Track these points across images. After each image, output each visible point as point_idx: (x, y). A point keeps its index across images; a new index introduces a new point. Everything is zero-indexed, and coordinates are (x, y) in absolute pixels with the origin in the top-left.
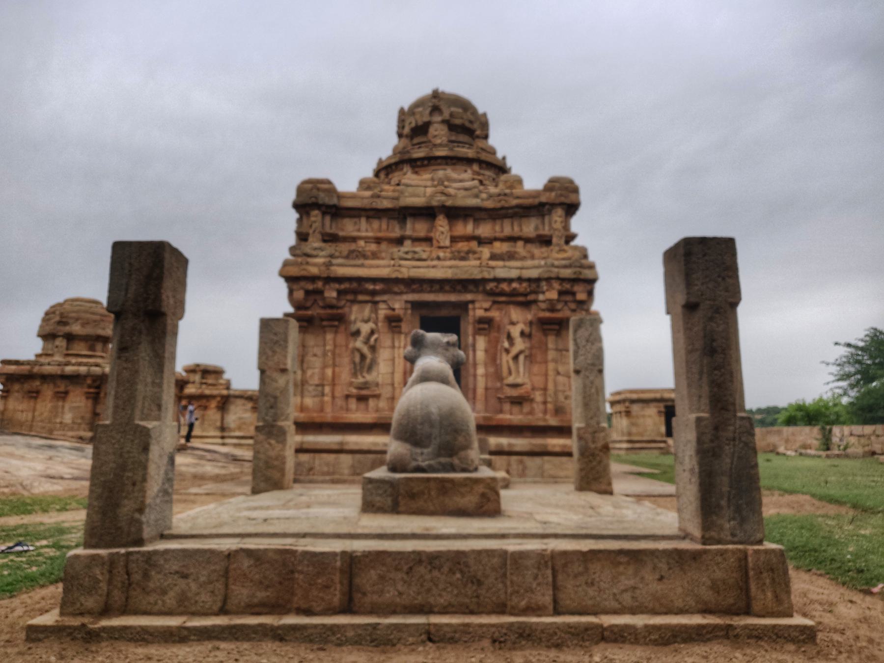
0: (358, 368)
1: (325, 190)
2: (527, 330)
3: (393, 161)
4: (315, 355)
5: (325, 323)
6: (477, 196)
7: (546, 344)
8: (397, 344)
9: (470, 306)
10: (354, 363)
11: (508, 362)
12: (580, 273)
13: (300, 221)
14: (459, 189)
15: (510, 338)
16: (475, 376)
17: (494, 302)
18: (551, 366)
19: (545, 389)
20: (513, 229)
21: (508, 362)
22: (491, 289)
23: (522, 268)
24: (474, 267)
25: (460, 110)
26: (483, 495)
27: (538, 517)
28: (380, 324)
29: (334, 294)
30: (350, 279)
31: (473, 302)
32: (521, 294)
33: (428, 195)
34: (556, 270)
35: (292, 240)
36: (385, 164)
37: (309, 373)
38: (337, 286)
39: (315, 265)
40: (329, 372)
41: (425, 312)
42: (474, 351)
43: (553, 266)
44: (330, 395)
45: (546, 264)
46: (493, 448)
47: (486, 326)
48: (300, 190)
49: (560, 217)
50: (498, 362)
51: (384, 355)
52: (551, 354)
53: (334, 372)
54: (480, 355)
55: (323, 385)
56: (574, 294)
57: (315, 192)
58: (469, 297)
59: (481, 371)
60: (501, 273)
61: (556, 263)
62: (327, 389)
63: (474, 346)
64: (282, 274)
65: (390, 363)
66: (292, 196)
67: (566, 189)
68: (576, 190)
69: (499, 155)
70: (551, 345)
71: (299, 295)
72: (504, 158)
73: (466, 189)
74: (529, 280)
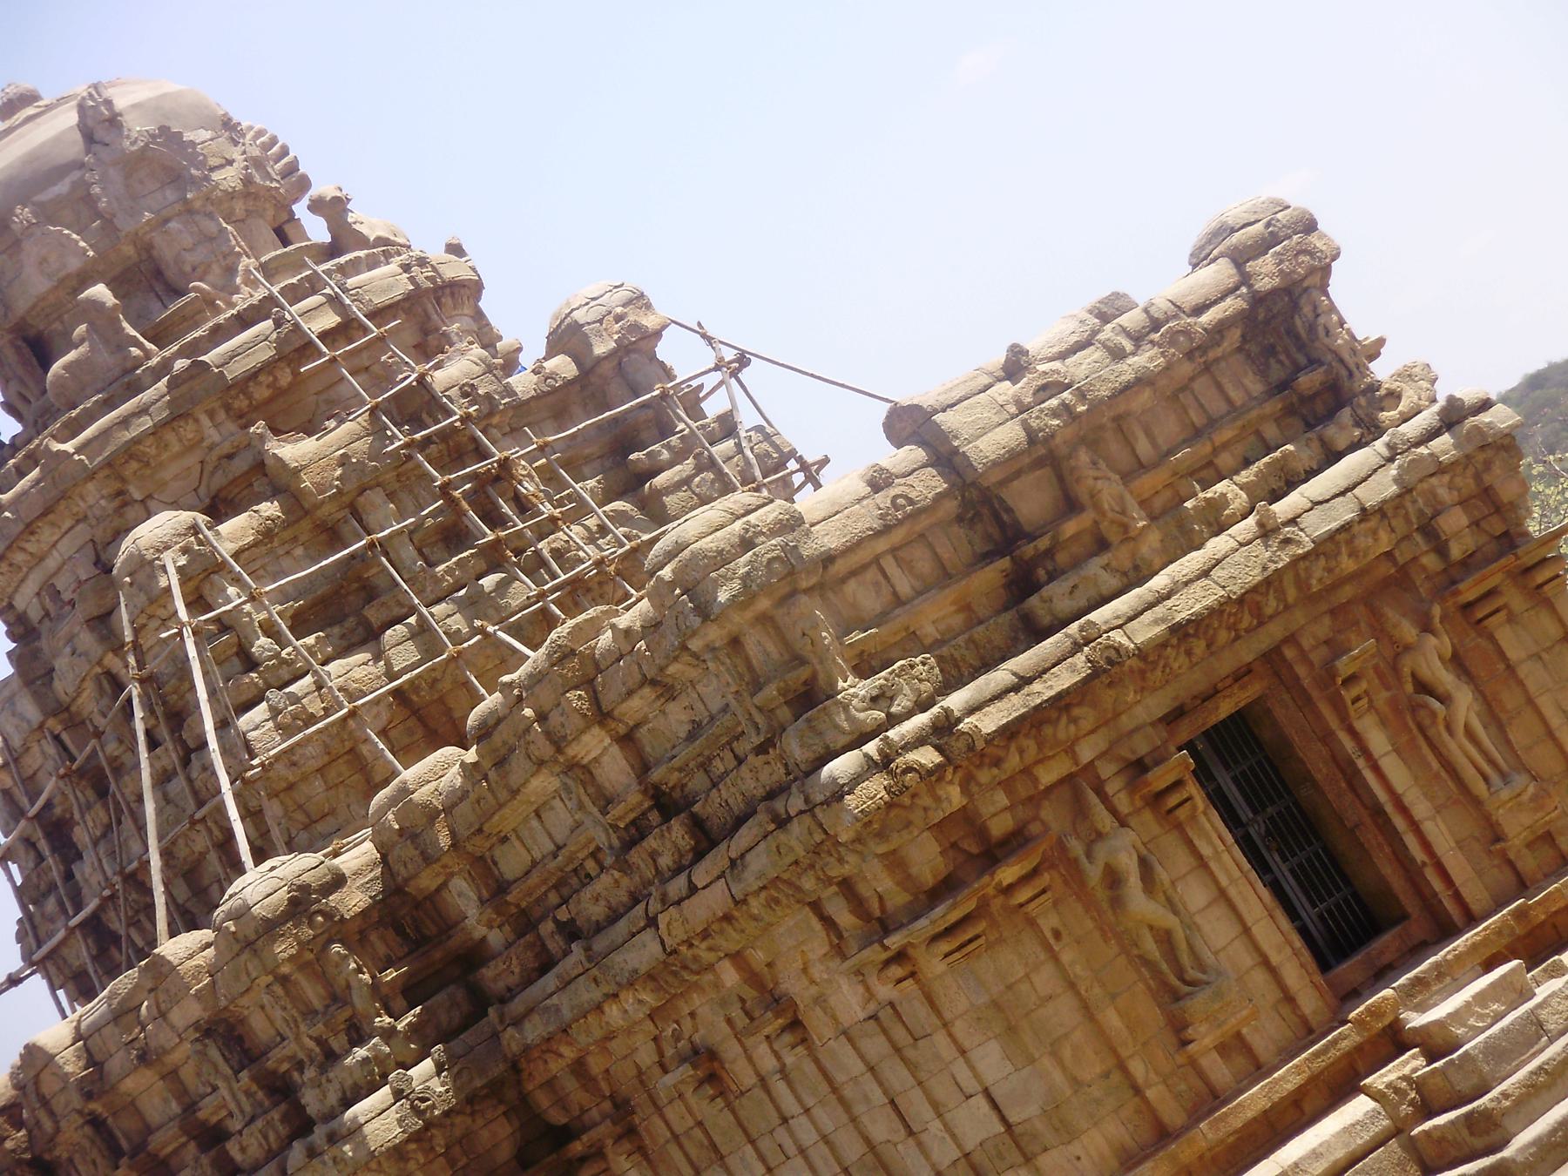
5: (1023, 895)
8: (1206, 851)
9: (1289, 653)
11: (1461, 747)
18: (1546, 704)
21: (1461, 747)
31: (1291, 639)
34: (1423, 450)
37: (1067, 1053)
51: (1195, 895)
59: (1421, 809)
60: (1319, 525)
65: (1220, 910)
70: (1513, 654)
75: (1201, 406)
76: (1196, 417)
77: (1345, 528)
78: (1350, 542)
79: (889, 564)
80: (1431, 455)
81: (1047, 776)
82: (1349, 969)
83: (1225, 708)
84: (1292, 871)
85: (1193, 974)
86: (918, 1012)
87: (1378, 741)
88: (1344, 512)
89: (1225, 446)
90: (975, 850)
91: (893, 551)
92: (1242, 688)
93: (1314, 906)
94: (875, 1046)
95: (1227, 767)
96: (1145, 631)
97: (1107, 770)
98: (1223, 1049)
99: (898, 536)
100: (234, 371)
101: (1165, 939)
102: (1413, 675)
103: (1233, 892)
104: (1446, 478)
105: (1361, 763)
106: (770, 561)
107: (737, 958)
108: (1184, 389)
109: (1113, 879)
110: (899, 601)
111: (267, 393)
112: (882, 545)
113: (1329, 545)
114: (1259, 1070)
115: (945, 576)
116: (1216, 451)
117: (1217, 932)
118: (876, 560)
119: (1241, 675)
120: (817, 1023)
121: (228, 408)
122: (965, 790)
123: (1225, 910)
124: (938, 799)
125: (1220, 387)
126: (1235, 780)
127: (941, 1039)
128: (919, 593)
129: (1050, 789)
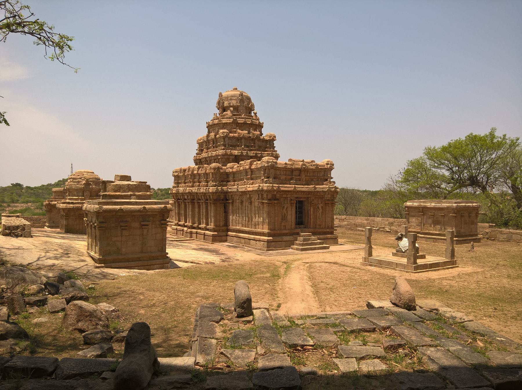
15: (318, 208)
30: (283, 191)
32: (320, 195)
39: (275, 187)
51: (289, 213)
52: (327, 212)
58: (310, 196)
59: (312, 217)
60: (317, 189)
81: (284, 196)
82: (298, 226)
83: (301, 200)
86: (261, 208)
87: (312, 210)
88: (321, 190)
94: (256, 209)
96: (251, 189)
97: (289, 198)
100: (239, 122)
101: (285, 215)
107: (250, 195)
113: (318, 192)
114: (286, 229)
115: (286, 175)
117: (289, 217)
119: (304, 198)
120: (253, 204)
123: (291, 215)
127: (262, 212)
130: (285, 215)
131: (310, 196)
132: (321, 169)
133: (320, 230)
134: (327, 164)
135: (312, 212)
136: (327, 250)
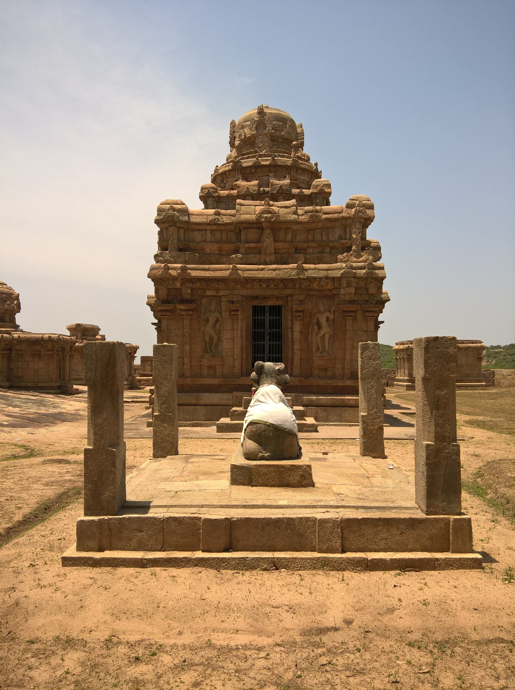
0: (208, 345)
1: (179, 211)
2: (332, 317)
3: (227, 169)
4: (176, 336)
5: (183, 313)
6: (295, 213)
7: (346, 328)
8: (235, 327)
9: (289, 298)
10: (205, 342)
12: (372, 273)
13: (160, 233)
14: (281, 207)
16: (293, 350)
17: (307, 295)
19: (344, 359)
20: (322, 238)
22: (305, 286)
23: (327, 270)
24: (292, 269)
25: (281, 124)
26: (302, 476)
27: (335, 489)
28: (223, 313)
29: (189, 291)
31: (291, 296)
33: (257, 212)
35: (155, 250)
36: (220, 171)
38: (191, 285)
39: (174, 269)
40: (187, 348)
41: (255, 303)
42: (292, 332)
43: (352, 268)
44: (188, 364)
45: (346, 266)
46: (305, 402)
47: (301, 314)
48: (160, 211)
49: (358, 229)
50: (310, 340)
51: (226, 335)
53: (190, 347)
54: (297, 335)
55: (183, 358)
56: (367, 289)
57: (171, 212)
59: (297, 346)
61: (354, 265)
62: (186, 360)
63: (292, 328)
64: (149, 277)
66: (154, 215)
67: (364, 205)
68: (371, 207)
69: (312, 162)
70: (348, 328)
71: (164, 292)
72: (316, 164)
73: (286, 207)
74: (333, 279)
75: (314, 236)
76: (310, 237)
77: (320, 278)
78: (320, 282)
79: (208, 233)
80: (355, 273)
81: (208, 293)
84: (270, 345)
85: (213, 349)
87: (297, 327)
88: (322, 274)
89: (312, 247)
90: (179, 299)
91: (212, 231)
92: (277, 300)
93: (270, 353)
95: (270, 315)
97: (224, 299)
98: (209, 367)
99: (214, 227)
100: (244, 165)
101: (211, 338)
102: (318, 319)
103: (235, 339)
104: (356, 280)
105: (290, 330)
106: (169, 216)
108: (311, 230)
109: (208, 321)
110: (205, 241)
111: (249, 172)
112: (208, 227)
113: (309, 279)
114: (215, 377)
115: (220, 241)
116: (308, 247)
117: (226, 345)
118: (206, 230)
119: (278, 298)
121: (241, 171)
122: (182, 284)
124: (174, 283)
125: (322, 234)
126: (270, 320)
128: (211, 242)
129: (208, 296)
130: (211, 338)
131: (288, 292)
132: (326, 219)
133: (322, 382)
134: (349, 206)
135: (297, 335)
136: (314, 435)
